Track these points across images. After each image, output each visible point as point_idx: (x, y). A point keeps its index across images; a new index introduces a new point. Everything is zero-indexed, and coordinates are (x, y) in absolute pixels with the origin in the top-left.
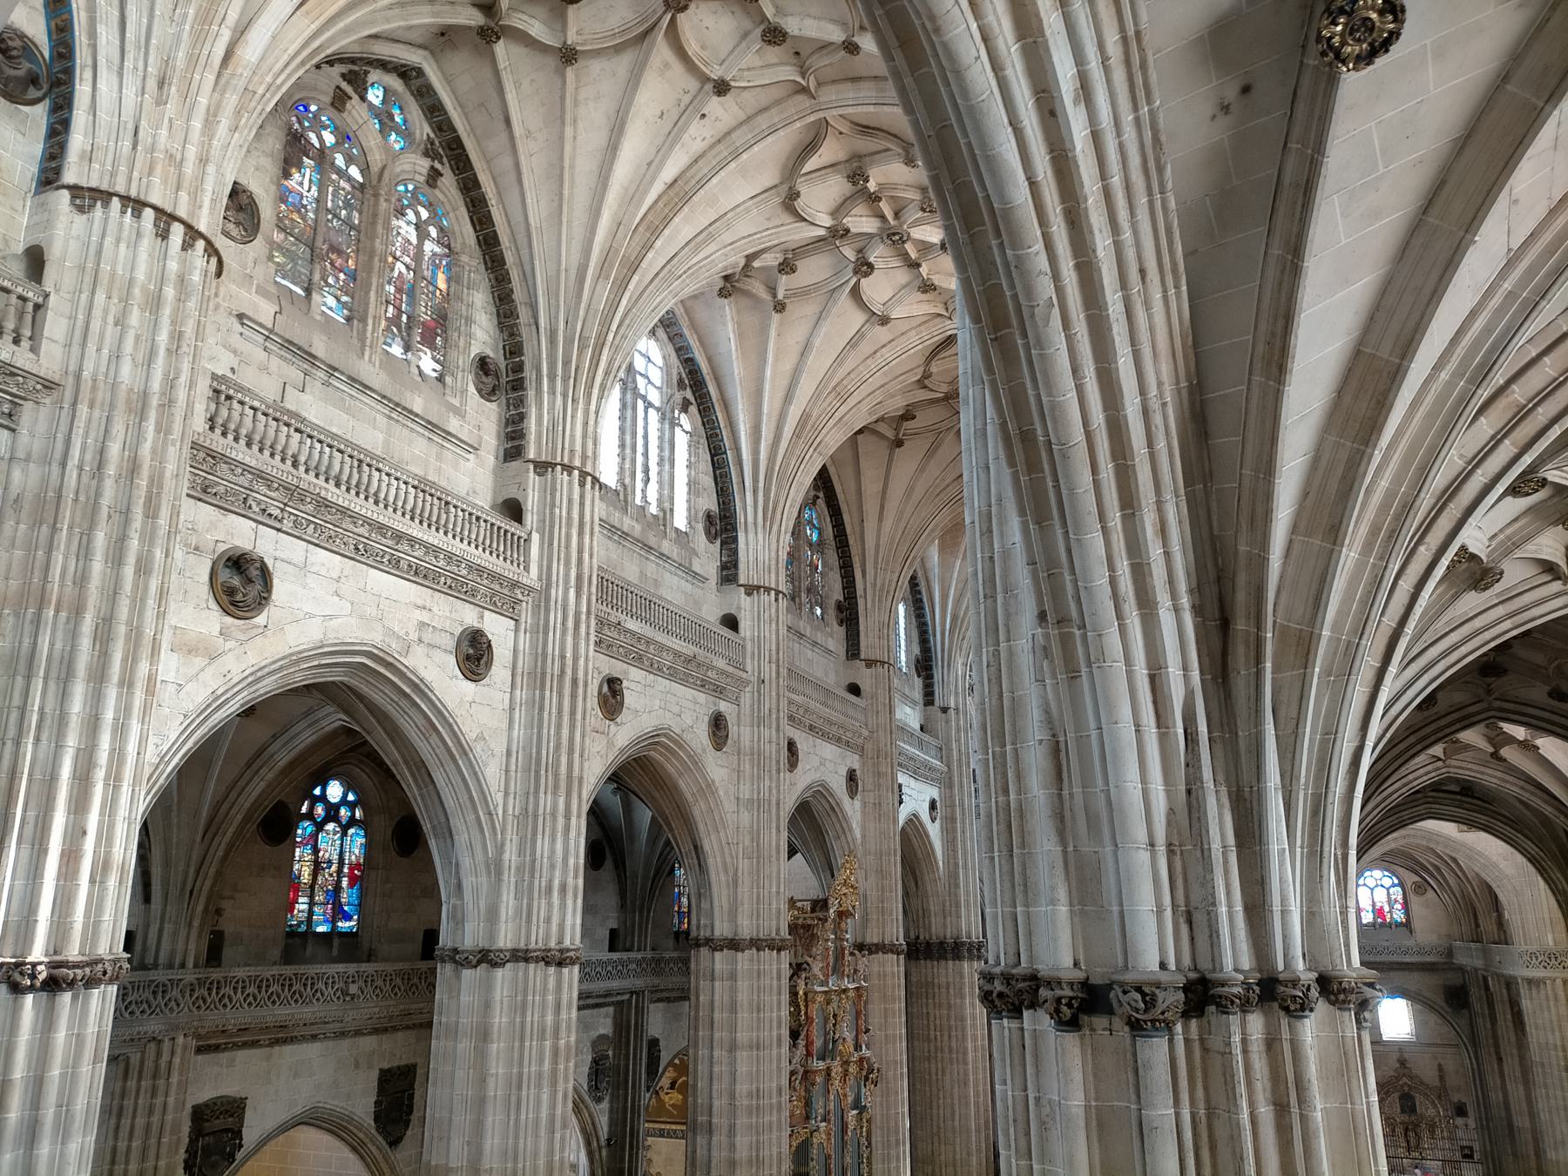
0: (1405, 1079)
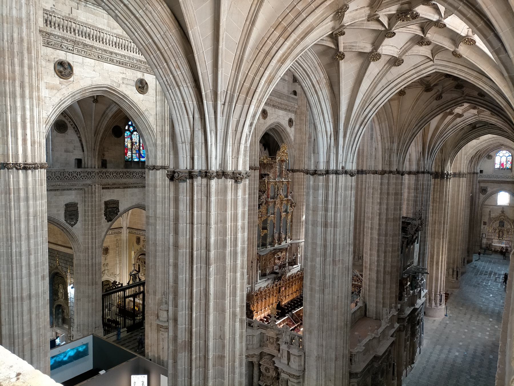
0: (502, 217)
